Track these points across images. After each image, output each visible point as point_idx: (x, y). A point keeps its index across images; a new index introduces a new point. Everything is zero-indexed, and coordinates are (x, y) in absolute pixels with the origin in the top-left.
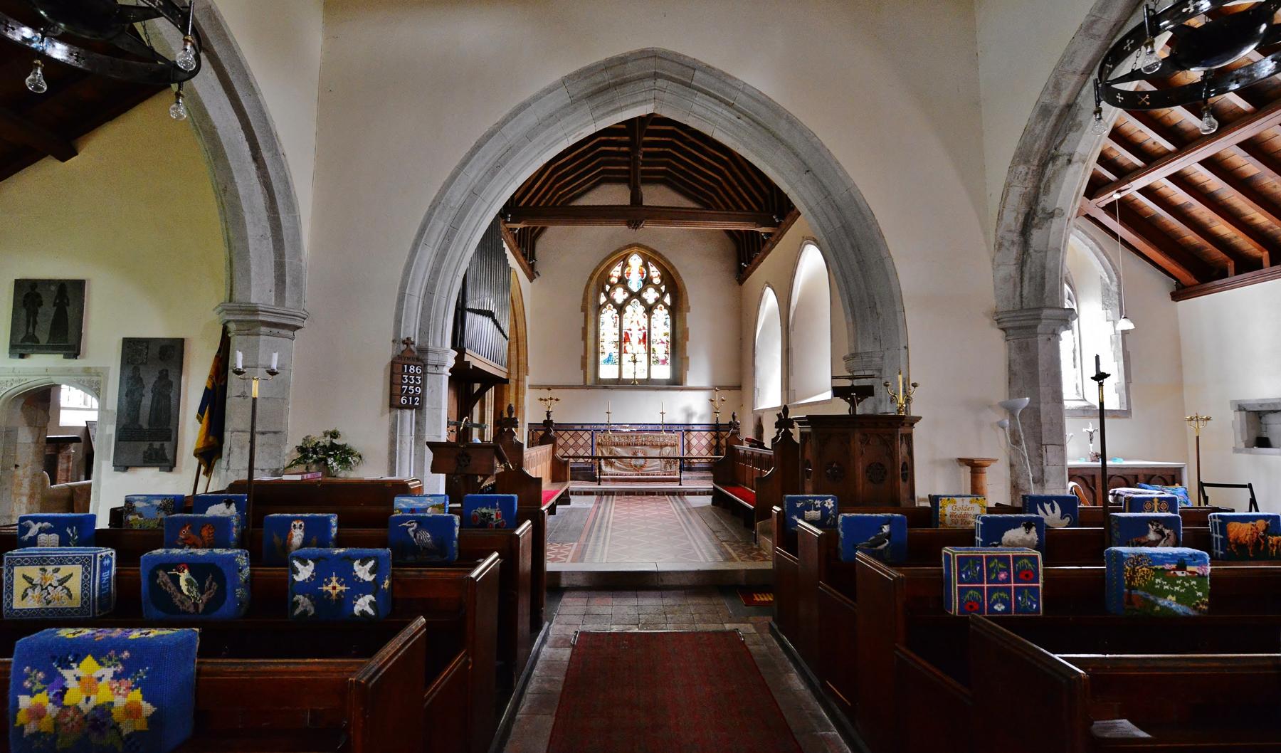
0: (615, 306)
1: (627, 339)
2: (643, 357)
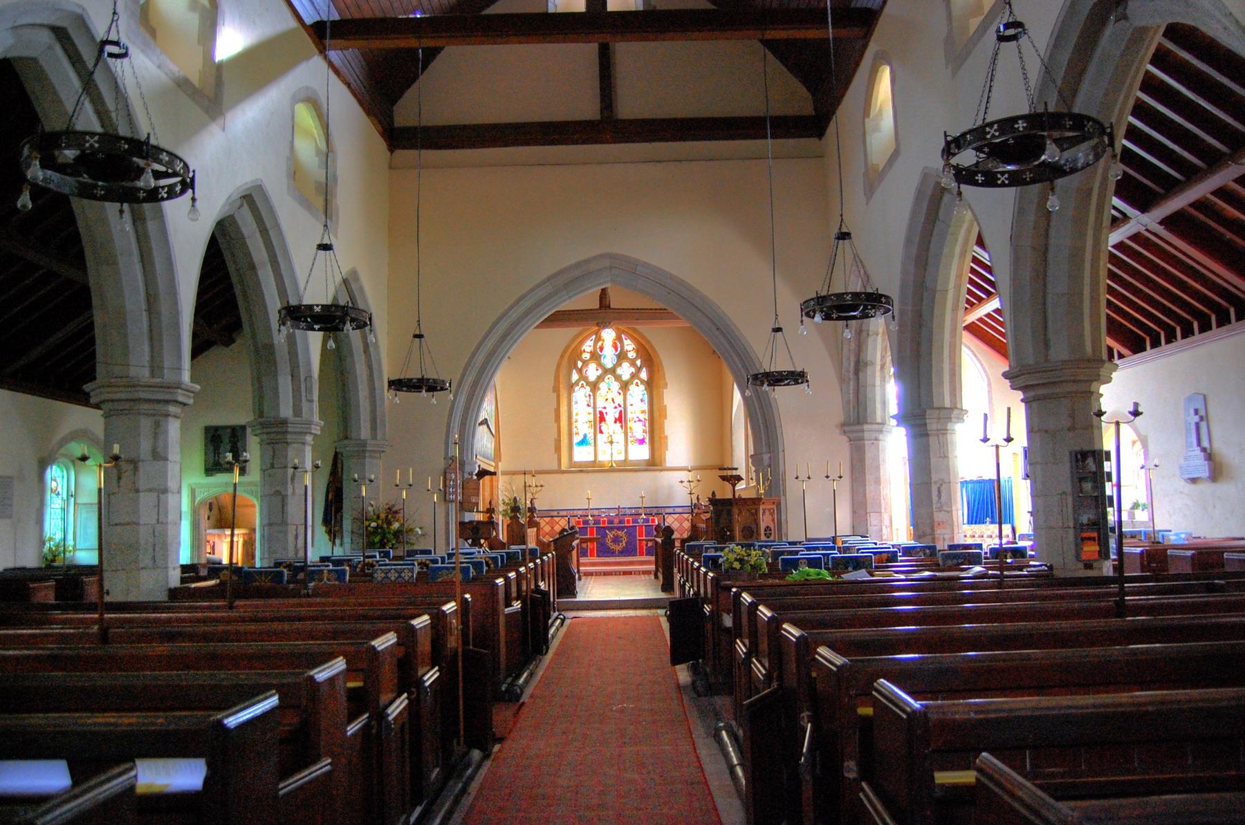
0: (588, 383)
1: (602, 419)
2: (619, 437)
